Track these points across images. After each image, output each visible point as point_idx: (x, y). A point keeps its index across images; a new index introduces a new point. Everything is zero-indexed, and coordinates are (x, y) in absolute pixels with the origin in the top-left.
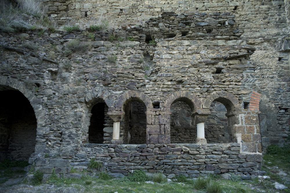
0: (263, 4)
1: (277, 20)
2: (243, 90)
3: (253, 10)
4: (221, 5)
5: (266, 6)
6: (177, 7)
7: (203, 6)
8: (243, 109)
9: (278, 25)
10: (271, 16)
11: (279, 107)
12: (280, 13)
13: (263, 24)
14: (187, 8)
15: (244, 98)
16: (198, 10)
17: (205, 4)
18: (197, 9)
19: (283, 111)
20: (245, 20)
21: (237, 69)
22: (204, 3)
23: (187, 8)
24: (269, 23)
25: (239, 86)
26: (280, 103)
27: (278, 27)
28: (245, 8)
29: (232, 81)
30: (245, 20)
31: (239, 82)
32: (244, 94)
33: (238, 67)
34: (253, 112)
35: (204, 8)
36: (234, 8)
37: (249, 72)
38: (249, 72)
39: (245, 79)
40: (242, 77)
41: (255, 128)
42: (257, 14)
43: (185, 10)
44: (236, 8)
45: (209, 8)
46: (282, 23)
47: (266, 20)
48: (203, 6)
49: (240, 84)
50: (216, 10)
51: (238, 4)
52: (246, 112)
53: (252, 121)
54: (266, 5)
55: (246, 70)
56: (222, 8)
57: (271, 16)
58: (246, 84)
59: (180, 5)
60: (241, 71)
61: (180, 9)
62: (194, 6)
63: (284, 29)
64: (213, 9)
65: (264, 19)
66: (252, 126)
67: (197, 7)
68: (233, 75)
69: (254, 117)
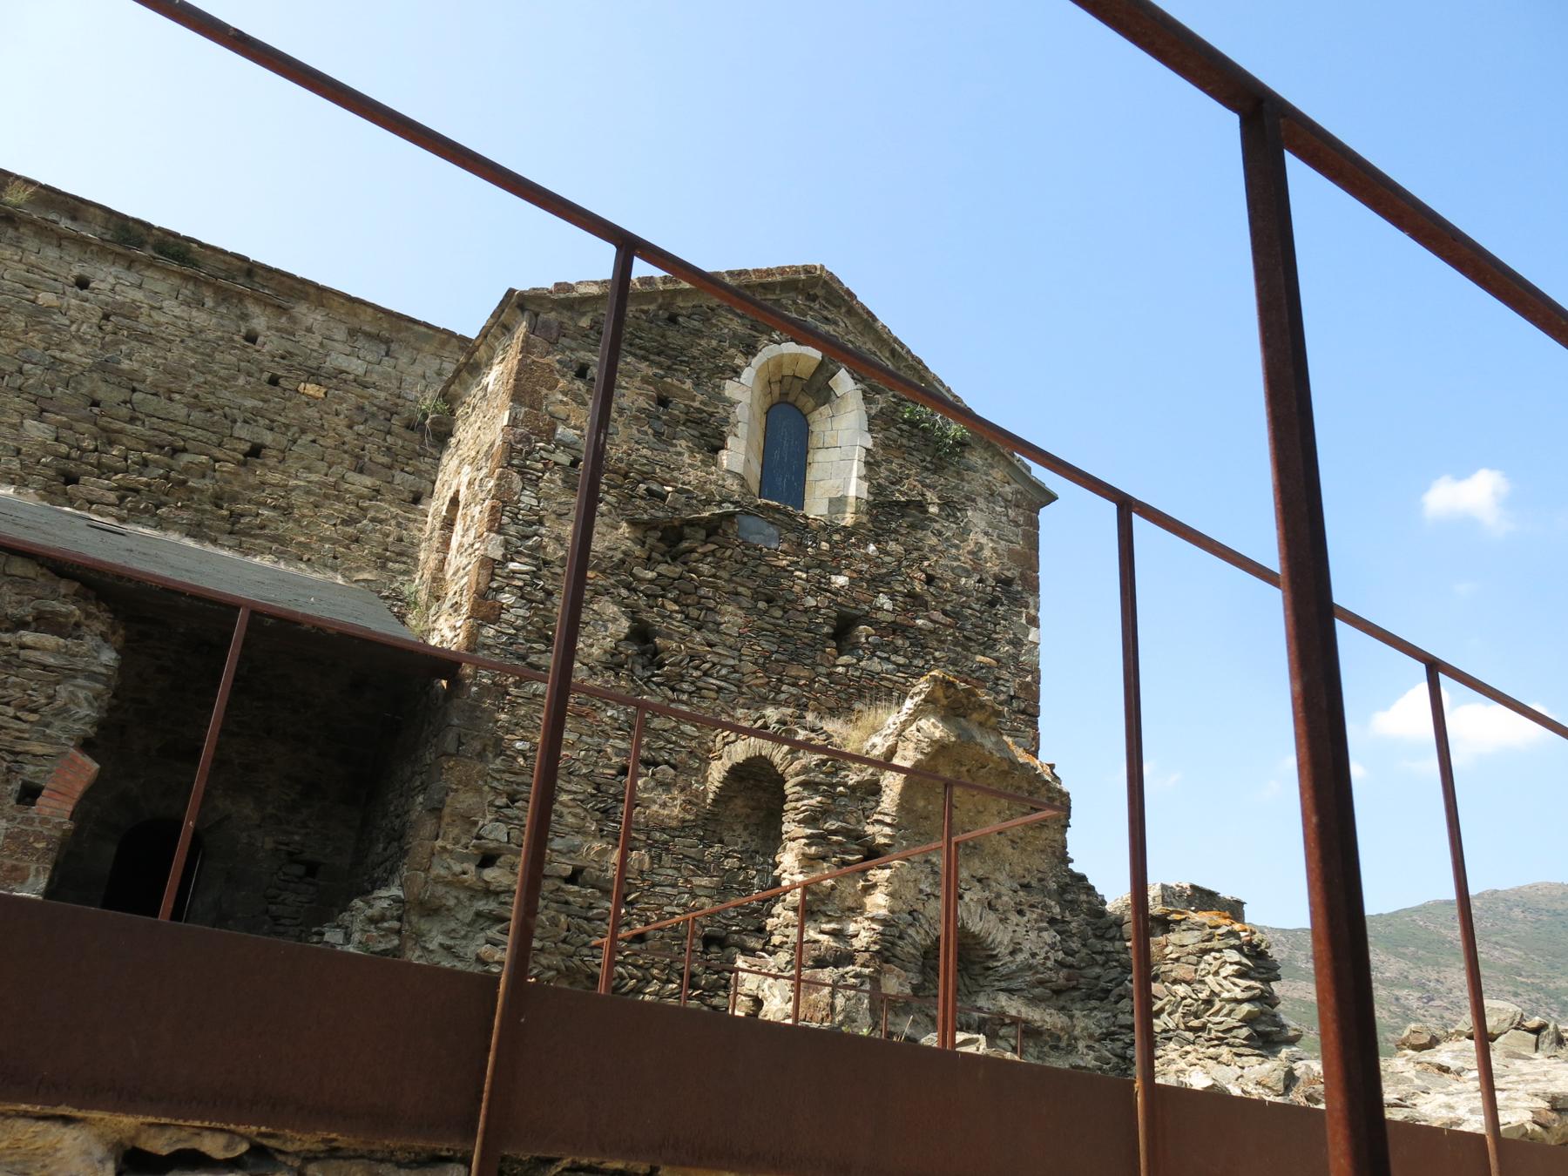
0: (361, 471)
1: (390, 539)
2: (37, 739)
3: (314, 477)
4: (199, 423)
5: (368, 481)
6: (9, 368)
7: (125, 402)
8: (13, 802)
9: (389, 559)
10: (373, 520)
11: (290, 854)
12: (408, 519)
13: (334, 542)
14: (53, 390)
15: (30, 769)
16: (96, 410)
17: (137, 396)
18: (95, 404)
19: (299, 870)
20: (274, 507)
21: (45, 667)
22: (134, 390)
23: (53, 390)
24: (357, 540)
25: (25, 726)
26: (297, 838)
27: (383, 567)
28: (289, 462)
29: (8, 704)
30: (274, 507)
31: (34, 711)
32: (35, 755)
33: (51, 661)
34: (44, 821)
35: (124, 411)
36: (246, 447)
37: (84, 688)
38: (84, 688)
39: (59, 703)
40: (51, 698)
41: (33, 872)
42: (326, 496)
43: (41, 392)
44: (256, 451)
45: (148, 415)
46: (400, 554)
47: (350, 530)
48: (125, 402)
49: (34, 717)
50: (171, 434)
51: (268, 438)
52: (20, 816)
53: (27, 848)
54: (371, 475)
55: (75, 677)
56: (199, 431)
57: (373, 520)
58: (57, 723)
59: (27, 367)
60: (52, 676)
61: (19, 382)
62: (84, 391)
63: (400, 578)
64: (164, 425)
65: (344, 522)
66: (22, 864)
67: (100, 395)
68: (15, 685)
69: (39, 837)
